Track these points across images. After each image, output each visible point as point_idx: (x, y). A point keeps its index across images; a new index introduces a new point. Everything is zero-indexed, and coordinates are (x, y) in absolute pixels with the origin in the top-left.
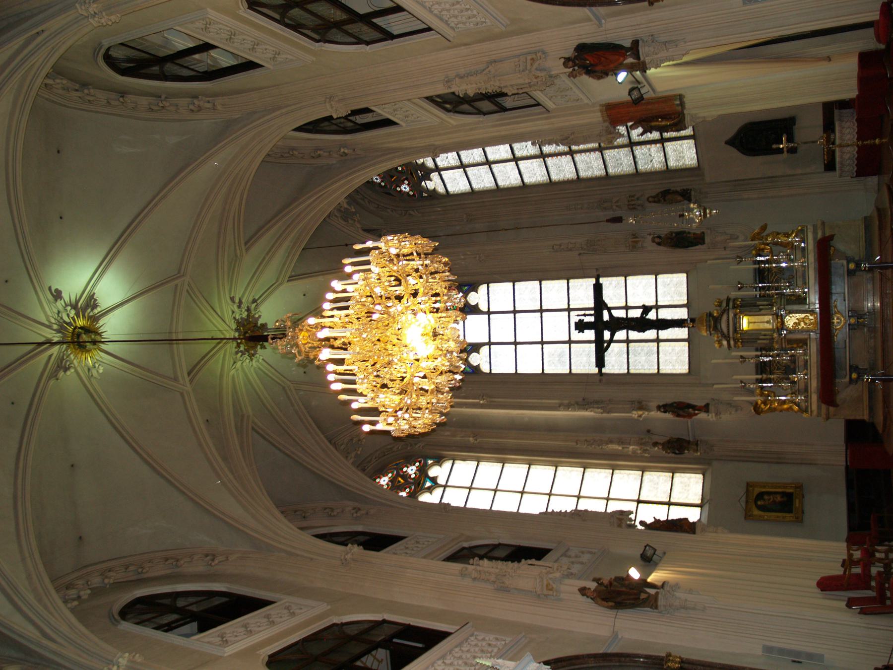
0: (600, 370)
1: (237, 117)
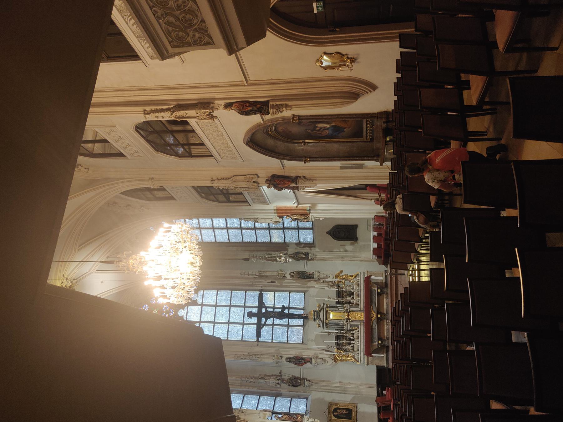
0: (258, 339)
1: (99, 179)
